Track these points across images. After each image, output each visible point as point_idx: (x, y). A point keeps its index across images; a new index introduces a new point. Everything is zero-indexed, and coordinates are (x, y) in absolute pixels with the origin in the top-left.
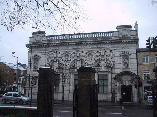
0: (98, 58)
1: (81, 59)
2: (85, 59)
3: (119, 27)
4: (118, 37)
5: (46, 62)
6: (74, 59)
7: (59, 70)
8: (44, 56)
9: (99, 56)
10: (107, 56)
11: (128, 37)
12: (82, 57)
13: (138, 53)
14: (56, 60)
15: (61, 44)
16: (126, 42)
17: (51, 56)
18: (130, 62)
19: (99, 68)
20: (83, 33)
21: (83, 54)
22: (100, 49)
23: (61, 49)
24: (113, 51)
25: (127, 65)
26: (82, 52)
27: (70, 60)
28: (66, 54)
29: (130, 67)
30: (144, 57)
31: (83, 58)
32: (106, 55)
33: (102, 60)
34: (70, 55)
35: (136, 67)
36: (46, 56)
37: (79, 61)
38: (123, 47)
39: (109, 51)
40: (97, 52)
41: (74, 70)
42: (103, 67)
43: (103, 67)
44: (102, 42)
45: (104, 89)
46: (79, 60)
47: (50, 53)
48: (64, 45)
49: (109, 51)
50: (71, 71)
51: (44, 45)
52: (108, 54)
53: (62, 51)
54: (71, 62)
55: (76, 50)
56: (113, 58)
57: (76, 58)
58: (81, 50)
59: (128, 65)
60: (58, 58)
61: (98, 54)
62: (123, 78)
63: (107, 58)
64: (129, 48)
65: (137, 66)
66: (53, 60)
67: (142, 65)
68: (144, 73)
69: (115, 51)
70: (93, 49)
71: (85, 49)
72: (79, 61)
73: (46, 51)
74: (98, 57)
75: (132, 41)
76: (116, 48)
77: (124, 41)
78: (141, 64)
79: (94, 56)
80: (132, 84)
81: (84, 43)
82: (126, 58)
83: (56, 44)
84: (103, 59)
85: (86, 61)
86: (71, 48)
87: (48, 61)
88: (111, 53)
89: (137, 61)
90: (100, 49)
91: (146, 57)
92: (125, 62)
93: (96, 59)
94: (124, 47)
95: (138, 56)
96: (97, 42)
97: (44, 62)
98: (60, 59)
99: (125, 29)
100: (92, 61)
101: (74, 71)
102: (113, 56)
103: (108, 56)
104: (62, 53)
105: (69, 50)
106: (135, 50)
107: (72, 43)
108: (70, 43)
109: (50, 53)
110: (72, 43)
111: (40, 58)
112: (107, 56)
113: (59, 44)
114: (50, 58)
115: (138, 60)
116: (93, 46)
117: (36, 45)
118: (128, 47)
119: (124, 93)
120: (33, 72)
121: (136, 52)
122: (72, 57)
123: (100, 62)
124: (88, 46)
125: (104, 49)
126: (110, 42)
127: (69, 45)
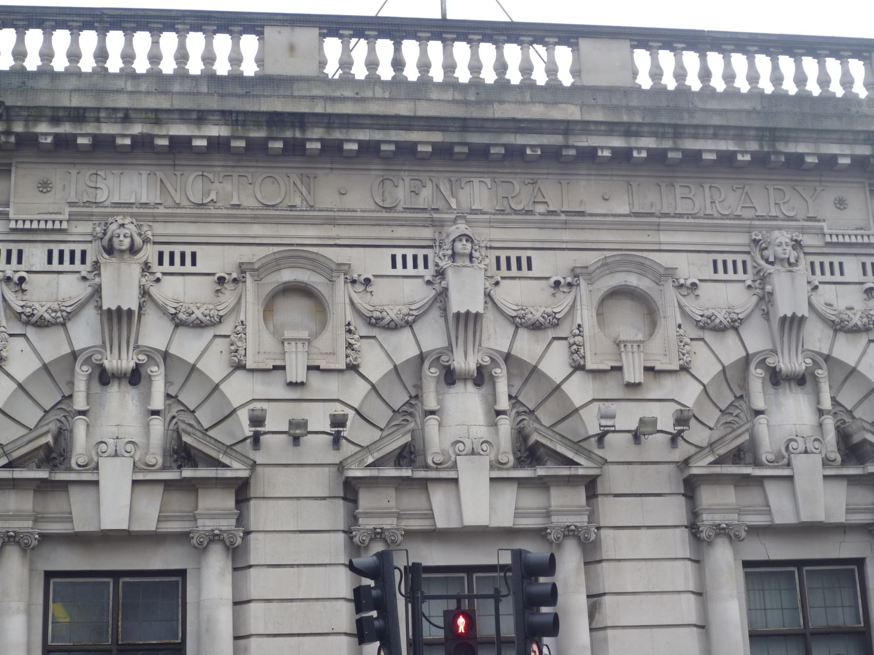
0: (730, 350)
1: (508, 357)
2: (559, 351)
6: (404, 347)
7: (179, 502)
9: (734, 326)
12: (521, 323)
14: (121, 361)
19: (761, 479)
20: (502, 18)
22: (742, 239)
23: (201, 212)
27: (353, 368)
28: (288, 275)
31: (527, 347)
32: (829, 313)
33: (776, 378)
34: (340, 296)
37: (481, 378)
39: (852, 269)
40: (709, 274)
41: (412, 501)
42: (808, 469)
43: (808, 469)
44: (782, 147)
46: (473, 366)
47: (36, 256)
48: (256, 150)
49: (852, 269)
50: (367, 523)
54: (356, 392)
55: (427, 233)
57: (431, 336)
58: (497, 234)
60: (154, 333)
61: (728, 297)
63: (847, 351)
66: (74, 355)
70: (654, 237)
71: (542, 225)
72: (481, 378)
74: (731, 338)
79: (671, 317)
83: (137, 129)
84: (791, 362)
85: (578, 390)
86: (355, 192)
90: (742, 239)
93: (706, 368)
98: (189, 347)
100: (666, 387)
101: (415, 524)
103: (855, 330)
104: (212, 260)
105: (332, 222)
107: (378, 136)
109: (36, 256)
113: (180, 130)
114: (41, 324)
122: (374, 322)
124: (587, 194)
125: (797, 245)
127: (332, 151)
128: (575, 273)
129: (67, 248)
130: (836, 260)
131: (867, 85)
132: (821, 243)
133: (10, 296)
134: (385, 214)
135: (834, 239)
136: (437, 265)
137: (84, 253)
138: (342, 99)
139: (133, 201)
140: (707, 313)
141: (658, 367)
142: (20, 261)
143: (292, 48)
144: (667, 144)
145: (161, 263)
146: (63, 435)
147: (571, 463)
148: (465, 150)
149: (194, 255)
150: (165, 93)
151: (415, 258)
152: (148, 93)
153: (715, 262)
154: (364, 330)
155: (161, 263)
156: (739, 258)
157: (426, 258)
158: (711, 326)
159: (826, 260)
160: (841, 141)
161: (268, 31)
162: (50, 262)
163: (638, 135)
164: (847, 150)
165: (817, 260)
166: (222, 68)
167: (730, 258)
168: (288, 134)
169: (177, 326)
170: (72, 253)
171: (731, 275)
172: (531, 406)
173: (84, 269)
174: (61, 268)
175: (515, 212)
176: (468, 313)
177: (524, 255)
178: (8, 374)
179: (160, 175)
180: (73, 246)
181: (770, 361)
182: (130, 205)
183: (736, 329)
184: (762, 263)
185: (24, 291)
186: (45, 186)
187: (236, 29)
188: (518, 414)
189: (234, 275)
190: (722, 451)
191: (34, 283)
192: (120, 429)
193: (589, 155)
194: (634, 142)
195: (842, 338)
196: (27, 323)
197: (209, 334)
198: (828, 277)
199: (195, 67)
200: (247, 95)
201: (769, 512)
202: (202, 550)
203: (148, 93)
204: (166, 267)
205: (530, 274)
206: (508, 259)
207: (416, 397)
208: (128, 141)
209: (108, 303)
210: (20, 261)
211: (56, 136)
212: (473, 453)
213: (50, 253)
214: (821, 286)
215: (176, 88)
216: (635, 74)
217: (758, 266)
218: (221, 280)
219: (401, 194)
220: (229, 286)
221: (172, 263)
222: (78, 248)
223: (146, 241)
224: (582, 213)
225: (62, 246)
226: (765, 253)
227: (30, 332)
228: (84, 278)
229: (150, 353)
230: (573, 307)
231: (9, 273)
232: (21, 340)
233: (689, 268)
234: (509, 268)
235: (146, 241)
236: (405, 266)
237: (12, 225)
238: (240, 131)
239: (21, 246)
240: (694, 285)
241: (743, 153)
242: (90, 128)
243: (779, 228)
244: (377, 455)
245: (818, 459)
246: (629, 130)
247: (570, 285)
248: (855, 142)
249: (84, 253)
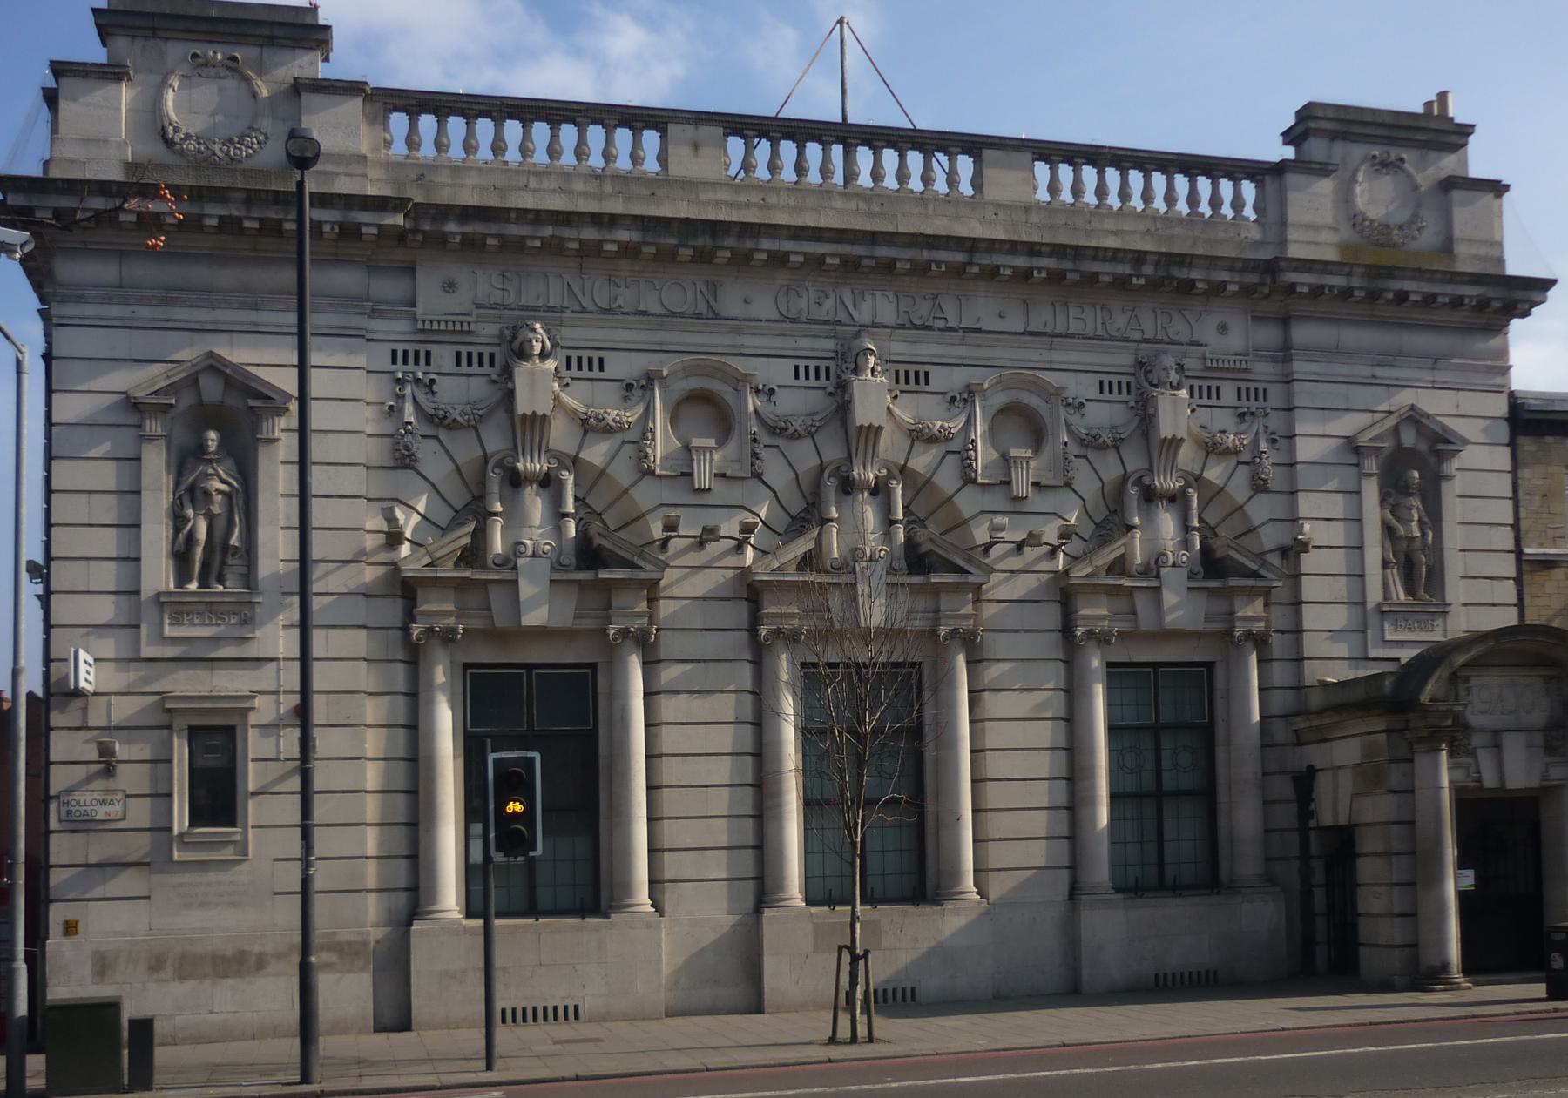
3: (1317, 126)
13: (1527, 445)
15: (624, 235)
18: (1454, 537)
20: (901, 122)
47: (443, 357)
48: (667, 257)
49: (1228, 393)
55: (830, 344)
72: (880, 490)
76: (1314, 367)
81: (942, 255)
83: (548, 231)
85: (967, 503)
86: (756, 300)
88: (1258, 425)
89: (1516, 527)
96: (1107, 267)
104: (621, 366)
105: (738, 332)
107: (788, 246)
108: (767, 244)
109: (443, 357)
110: (788, 246)
113: (589, 234)
115: (1523, 514)
116: (1042, 318)
117: (213, 213)
124: (985, 309)
125: (1181, 368)
130: (1214, 384)
131: (1256, 208)
133: (422, 398)
136: (839, 377)
137: (492, 356)
138: (748, 205)
139: (540, 303)
140: (1094, 432)
142: (428, 363)
144: (1067, 265)
145: (569, 367)
148: (872, 263)
149: (601, 360)
150: (568, 192)
151: (817, 368)
152: (553, 191)
153: (1101, 382)
154: (765, 439)
155: (569, 367)
156: (1125, 379)
159: (1205, 384)
161: (672, 128)
162: (458, 363)
163: (1039, 254)
166: (623, 163)
167: (1115, 379)
168: (700, 242)
169: (586, 432)
170: (481, 355)
171: (1115, 396)
172: (921, 515)
173: (494, 373)
174: (469, 370)
176: (870, 426)
177: (922, 369)
178: (421, 475)
179: (567, 278)
181: (1146, 480)
184: (1146, 385)
185: (433, 393)
186: (450, 287)
187: (638, 125)
188: (909, 522)
189: (643, 382)
193: (992, 273)
196: (440, 425)
198: (1205, 401)
199: (596, 161)
203: (553, 191)
204: (574, 372)
205: (927, 388)
206: (907, 373)
207: (813, 504)
208: (538, 244)
210: (428, 363)
211: (463, 235)
213: (458, 354)
215: (579, 186)
216: (1036, 189)
218: (629, 387)
219: (803, 303)
220: (637, 392)
221: (580, 368)
222: (486, 351)
224: (979, 331)
225: (470, 348)
226: (1150, 376)
227: (443, 434)
228: (494, 382)
231: (420, 375)
232: (433, 442)
234: (907, 382)
236: (807, 377)
237: (420, 325)
238: (649, 239)
239: (429, 347)
240: (1081, 405)
246: (1032, 249)
247: (965, 400)
249: (492, 356)
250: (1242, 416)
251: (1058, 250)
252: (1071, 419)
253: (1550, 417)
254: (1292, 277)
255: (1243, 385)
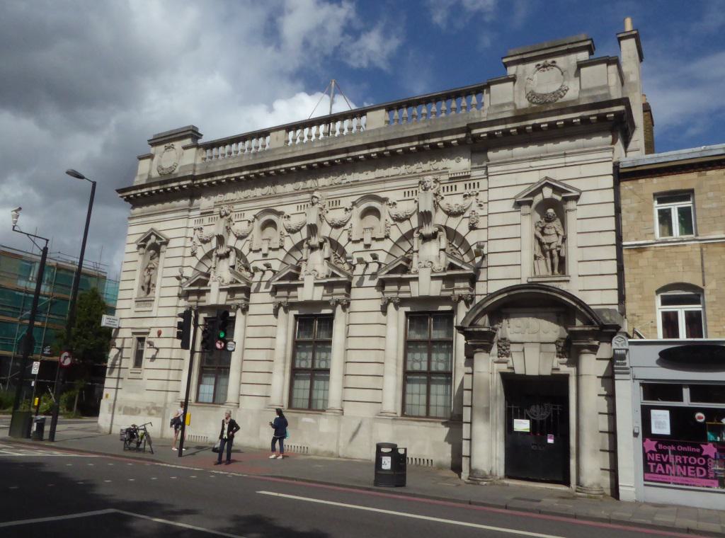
4: (506, 108)
5: (188, 262)
8: (182, 233)
9: (407, 218)
10: (451, 214)
11: (560, 100)
13: (626, 186)
16: (552, 125)
17: (209, 231)
21: (338, 215)
24: (484, 184)
25: (556, 260)
26: (335, 204)
29: (573, 267)
30: (664, 206)
35: (612, 267)
36: (190, 233)
38: (535, 159)
42: (424, 275)
44: (427, 141)
45: (424, 398)
51: (182, 183)
52: (455, 201)
53: (245, 207)
56: (482, 223)
59: (562, 261)
62: (512, 328)
63: (453, 223)
64: (568, 159)
65: (620, 259)
67: (648, 254)
68: (666, 301)
69: (494, 181)
73: (192, 213)
74: (406, 222)
75: (585, 120)
77: (537, 121)
78: (640, 249)
80: (564, 369)
82: (549, 220)
84: (428, 230)
85: (350, 249)
87: (194, 254)
88: (473, 199)
90: (416, 181)
91: (674, 208)
92: (544, 239)
94: (540, 158)
95: (625, 204)
97: (178, 262)
99: (549, 61)
102: (481, 212)
106: (609, 168)
111: (166, 243)
112: (451, 214)
115: (624, 223)
118: (565, 155)
119: (522, 425)
120: (137, 306)
121: (609, 181)
123: (415, 249)
126: (462, 136)
128: (255, 216)
129: (472, 182)
130: (454, 185)
132: (448, 178)
134: (296, 192)
135: (453, 176)
141: (377, 237)
143: (277, 139)
144: (383, 149)
146: (409, 261)
147: (460, 268)
157: (416, 191)
158: (399, 219)
159: (449, 185)
160: (452, 134)
164: (454, 137)
165: (445, 186)
167: (410, 190)
175: (336, 184)
180: (474, 181)
182: (228, 200)
183: (409, 219)
190: (391, 269)
191: (205, 229)
192: (317, 264)
194: (371, 151)
195: (451, 219)
197: (245, 240)
198: (450, 192)
200: (263, 157)
201: (410, 292)
202: (334, 308)
209: (422, 210)
212: (425, 267)
214: (445, 197)
215: (244, 159)
217: (409, 193)
223: (231, 212)
224: (358, 181)
229: (231, 248)
230: (350, 218)
233: (393, 196)
235: (231, 212)
241: (412, 147)
242: (215, 179)
243: (428, 175)
244: (280, 277)
245: (429, 270)
248: (457, 133)
250: (465, 196)
251: (379, 144)
252: (390, 210)
253: (638, 169)
254: (475, 131)
255: (468, 183)
